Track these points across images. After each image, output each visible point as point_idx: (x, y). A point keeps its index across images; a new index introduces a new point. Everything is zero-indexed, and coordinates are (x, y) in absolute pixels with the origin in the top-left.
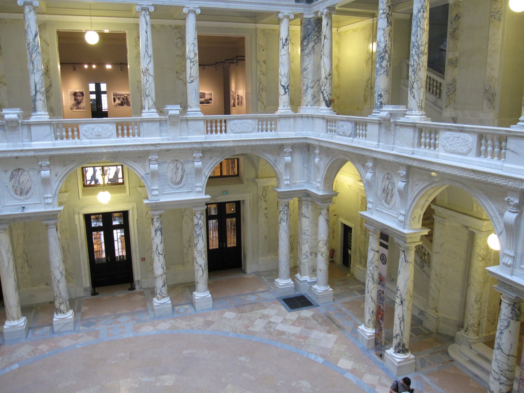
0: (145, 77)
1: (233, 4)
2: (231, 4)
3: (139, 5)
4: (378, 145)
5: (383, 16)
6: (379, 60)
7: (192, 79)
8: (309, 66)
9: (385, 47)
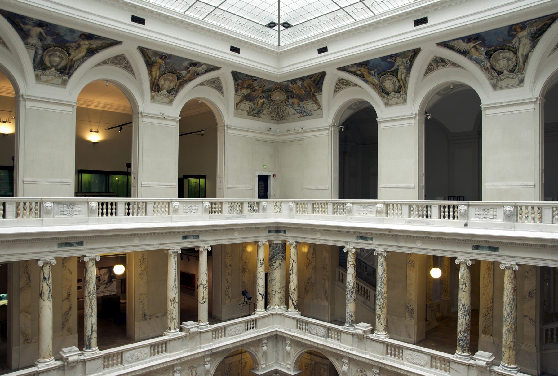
0: (173, 305)
1: (232, 240)
2: (230, 240)
3: (171, 250)
4: (352, 348)
5: (352, 266)
6: (350, 293)
7: (204, 300)
8: (277, 277)
9: (354, 285)
